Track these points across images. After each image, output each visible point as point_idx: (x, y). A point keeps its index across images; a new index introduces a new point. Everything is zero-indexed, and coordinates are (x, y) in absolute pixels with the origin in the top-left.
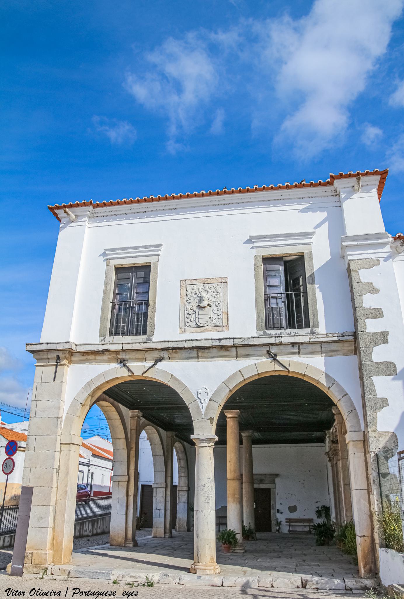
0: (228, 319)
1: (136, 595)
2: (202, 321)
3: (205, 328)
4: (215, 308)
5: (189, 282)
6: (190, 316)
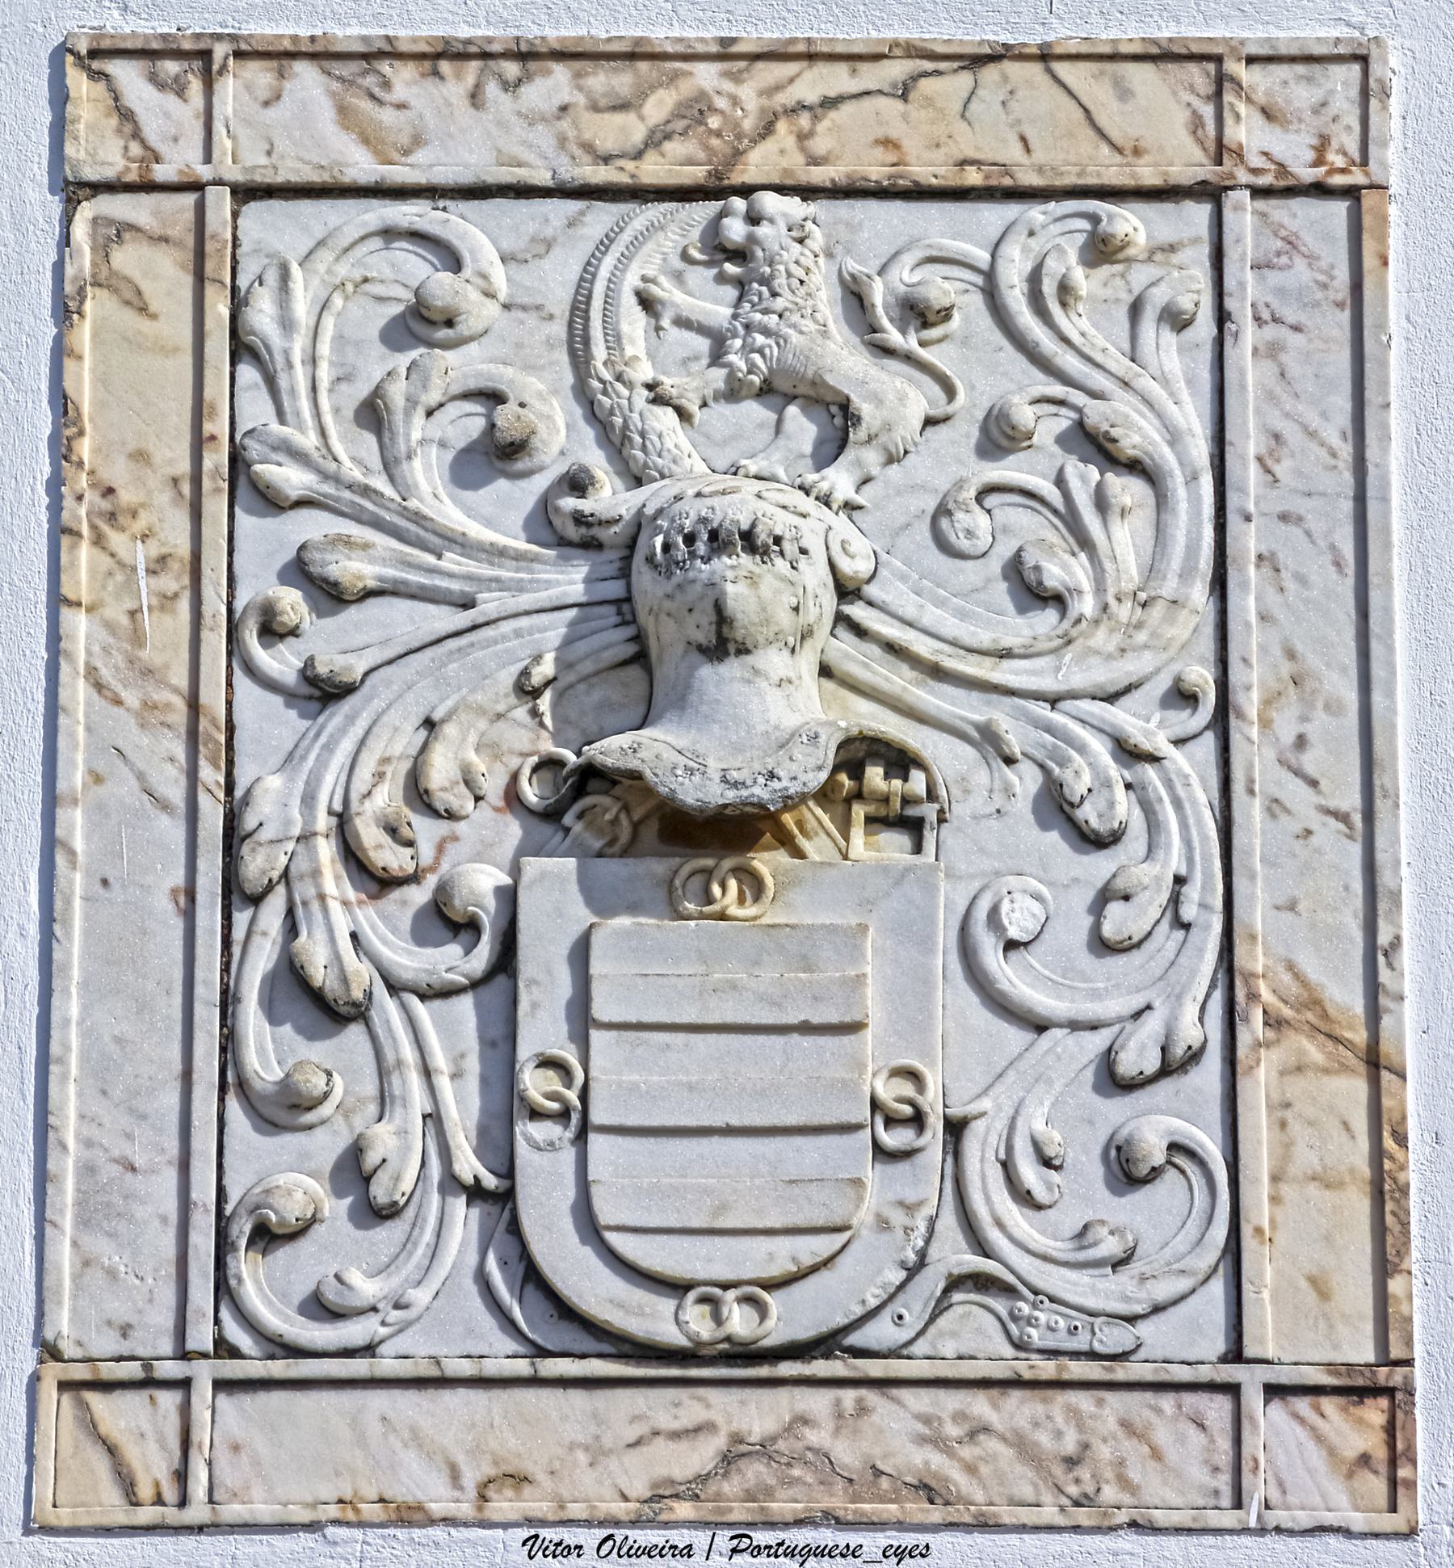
0: (1384, 1190)
1: (923, 1556)
2: (678, 1191)
3: (756, 1413)
4: (1039, 888)
5: (305, 124)
6: (336, 1064)
